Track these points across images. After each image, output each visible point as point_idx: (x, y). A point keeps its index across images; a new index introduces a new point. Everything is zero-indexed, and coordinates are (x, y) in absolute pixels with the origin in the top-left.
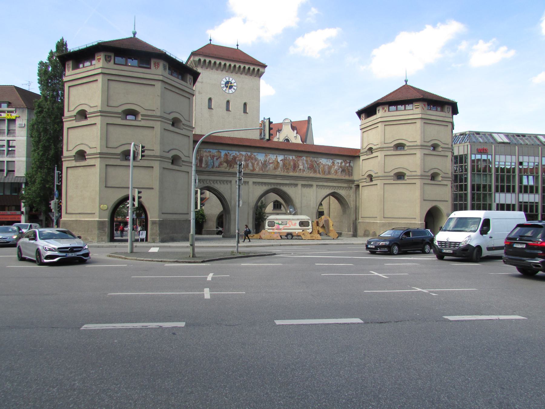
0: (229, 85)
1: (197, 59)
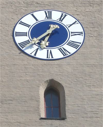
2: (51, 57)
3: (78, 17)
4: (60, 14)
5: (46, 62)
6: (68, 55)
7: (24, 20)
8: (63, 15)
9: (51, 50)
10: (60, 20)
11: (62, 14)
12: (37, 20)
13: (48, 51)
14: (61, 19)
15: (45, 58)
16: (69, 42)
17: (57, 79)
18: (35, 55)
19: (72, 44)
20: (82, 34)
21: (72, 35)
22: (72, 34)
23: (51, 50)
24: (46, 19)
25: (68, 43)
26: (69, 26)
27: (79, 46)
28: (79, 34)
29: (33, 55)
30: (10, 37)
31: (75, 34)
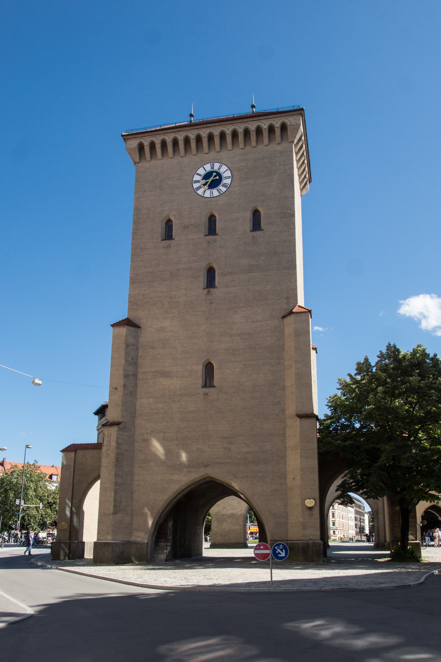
1: (134, 143)
2: (212, 196)
8: (221, 165)
11: (220, 164)
12: (206, 171)
14: (219, 169)
19: (224, 186)
21: (225, 179)
28: (228, 178)
29: (202, 195)
31: (227, 178)
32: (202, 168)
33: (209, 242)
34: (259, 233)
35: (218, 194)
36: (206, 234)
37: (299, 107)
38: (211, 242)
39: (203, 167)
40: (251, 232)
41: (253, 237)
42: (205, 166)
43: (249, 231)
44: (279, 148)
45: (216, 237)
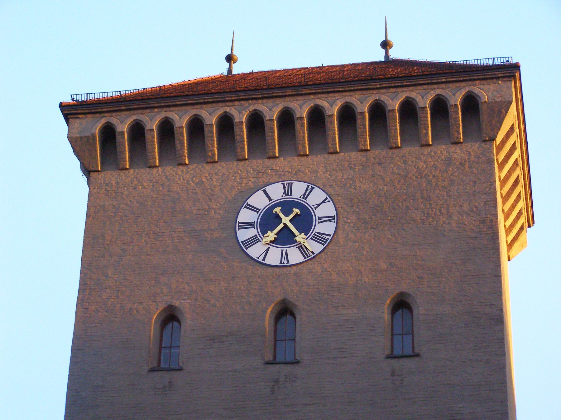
0: (286, 220)
2: (286, 262)
3: (330, 191)
4: (304, 186)
5: (277, 270)
6: (310, 256)
7: (251, 201)
8: (310, 187)
9: (286, 250)
10: (303, 198)
11: (308, 186)
12: (270, 199)
13: (282, 251)
14: (305, 196)
15: (277, 263)
16: (314, 234)
17: (292, 298)
18: (264, 260)
20: (334, 219)
21: (319, 223)
22: (320, 221)
23: (286, 250)
24: (284, 197)
25: (313, 236)
26: (315, 206)
27: (327, 240)
29: (260, 260)
30: (230, 231)
31: (323, 220)
32: (260, 193)
33: (277, 381)
34: (409, 363)
35: (301, 259)
36: (266, 360)
37: (507, 61)
38: (282, 379)
39: (265, 191)
40: (389, 360)
41: (393, 373)
42: (268, 189)
43: (384, 356)
44: (458, 153)
45: (298, 370)
